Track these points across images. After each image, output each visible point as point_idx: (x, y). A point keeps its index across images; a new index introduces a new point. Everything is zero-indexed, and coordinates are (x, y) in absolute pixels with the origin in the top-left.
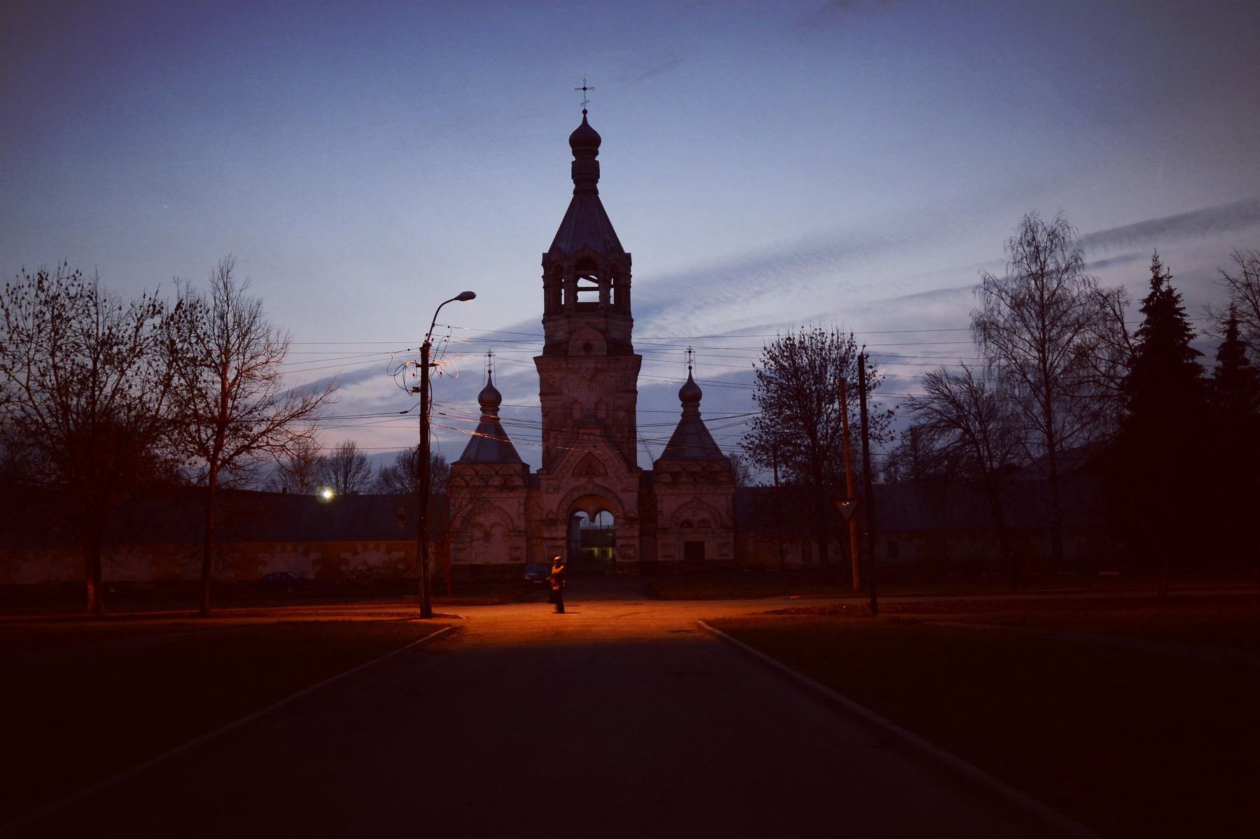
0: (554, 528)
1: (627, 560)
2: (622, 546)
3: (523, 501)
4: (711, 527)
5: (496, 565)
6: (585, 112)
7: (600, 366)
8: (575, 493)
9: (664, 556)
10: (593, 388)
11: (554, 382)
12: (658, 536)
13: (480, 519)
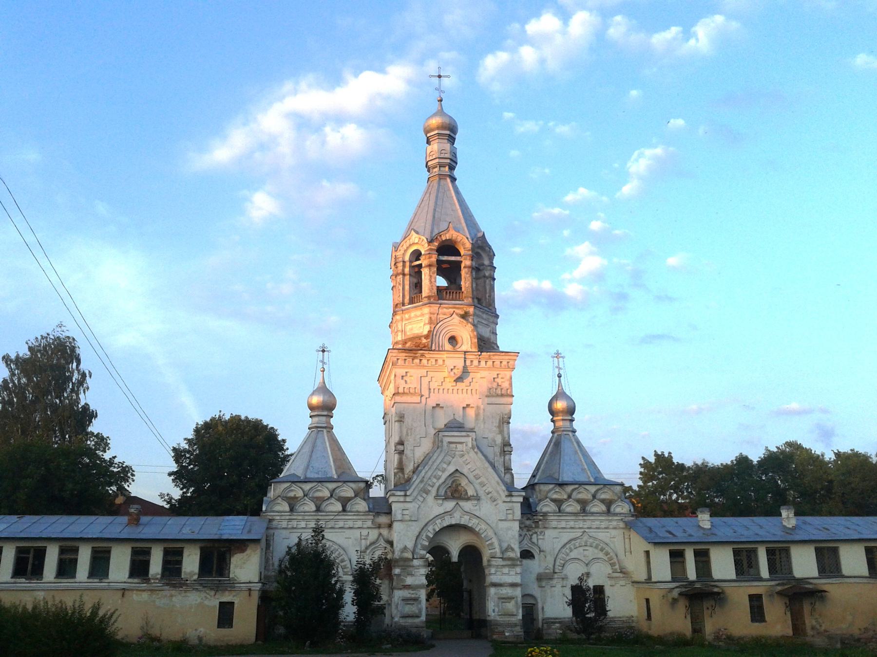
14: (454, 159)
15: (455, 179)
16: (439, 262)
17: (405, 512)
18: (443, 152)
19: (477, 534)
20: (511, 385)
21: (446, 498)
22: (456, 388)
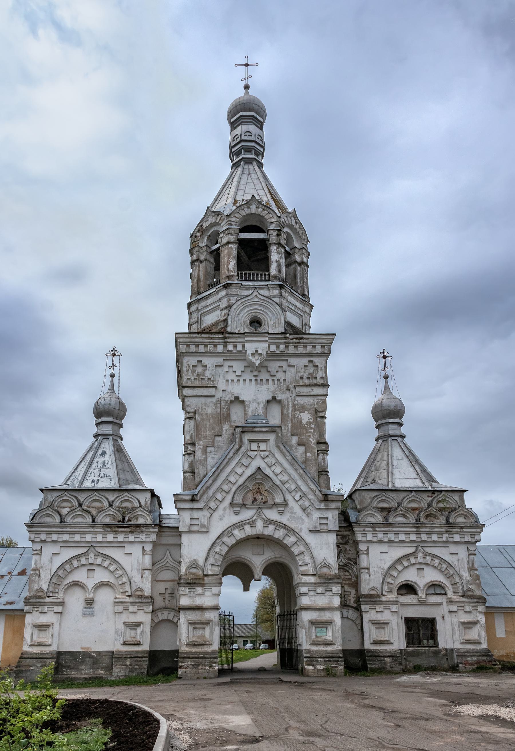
0: (199, 590)
1: (322, 648)
2: (313, 622)
3: (149, 548)
4: (445, 594)
5: (99, 653)
7: (273, 348)
9: (376, 642)
10: (262, 380)
11: (205, 371)
12: (363, 607)
13: (80, 576)
14: (260, 142)
15: (262, 165)
17: (195, 522)
18: (248, 134)
19: (286, 548)
20: (326, 372)
21: (243, 505)
22: (259, 379)
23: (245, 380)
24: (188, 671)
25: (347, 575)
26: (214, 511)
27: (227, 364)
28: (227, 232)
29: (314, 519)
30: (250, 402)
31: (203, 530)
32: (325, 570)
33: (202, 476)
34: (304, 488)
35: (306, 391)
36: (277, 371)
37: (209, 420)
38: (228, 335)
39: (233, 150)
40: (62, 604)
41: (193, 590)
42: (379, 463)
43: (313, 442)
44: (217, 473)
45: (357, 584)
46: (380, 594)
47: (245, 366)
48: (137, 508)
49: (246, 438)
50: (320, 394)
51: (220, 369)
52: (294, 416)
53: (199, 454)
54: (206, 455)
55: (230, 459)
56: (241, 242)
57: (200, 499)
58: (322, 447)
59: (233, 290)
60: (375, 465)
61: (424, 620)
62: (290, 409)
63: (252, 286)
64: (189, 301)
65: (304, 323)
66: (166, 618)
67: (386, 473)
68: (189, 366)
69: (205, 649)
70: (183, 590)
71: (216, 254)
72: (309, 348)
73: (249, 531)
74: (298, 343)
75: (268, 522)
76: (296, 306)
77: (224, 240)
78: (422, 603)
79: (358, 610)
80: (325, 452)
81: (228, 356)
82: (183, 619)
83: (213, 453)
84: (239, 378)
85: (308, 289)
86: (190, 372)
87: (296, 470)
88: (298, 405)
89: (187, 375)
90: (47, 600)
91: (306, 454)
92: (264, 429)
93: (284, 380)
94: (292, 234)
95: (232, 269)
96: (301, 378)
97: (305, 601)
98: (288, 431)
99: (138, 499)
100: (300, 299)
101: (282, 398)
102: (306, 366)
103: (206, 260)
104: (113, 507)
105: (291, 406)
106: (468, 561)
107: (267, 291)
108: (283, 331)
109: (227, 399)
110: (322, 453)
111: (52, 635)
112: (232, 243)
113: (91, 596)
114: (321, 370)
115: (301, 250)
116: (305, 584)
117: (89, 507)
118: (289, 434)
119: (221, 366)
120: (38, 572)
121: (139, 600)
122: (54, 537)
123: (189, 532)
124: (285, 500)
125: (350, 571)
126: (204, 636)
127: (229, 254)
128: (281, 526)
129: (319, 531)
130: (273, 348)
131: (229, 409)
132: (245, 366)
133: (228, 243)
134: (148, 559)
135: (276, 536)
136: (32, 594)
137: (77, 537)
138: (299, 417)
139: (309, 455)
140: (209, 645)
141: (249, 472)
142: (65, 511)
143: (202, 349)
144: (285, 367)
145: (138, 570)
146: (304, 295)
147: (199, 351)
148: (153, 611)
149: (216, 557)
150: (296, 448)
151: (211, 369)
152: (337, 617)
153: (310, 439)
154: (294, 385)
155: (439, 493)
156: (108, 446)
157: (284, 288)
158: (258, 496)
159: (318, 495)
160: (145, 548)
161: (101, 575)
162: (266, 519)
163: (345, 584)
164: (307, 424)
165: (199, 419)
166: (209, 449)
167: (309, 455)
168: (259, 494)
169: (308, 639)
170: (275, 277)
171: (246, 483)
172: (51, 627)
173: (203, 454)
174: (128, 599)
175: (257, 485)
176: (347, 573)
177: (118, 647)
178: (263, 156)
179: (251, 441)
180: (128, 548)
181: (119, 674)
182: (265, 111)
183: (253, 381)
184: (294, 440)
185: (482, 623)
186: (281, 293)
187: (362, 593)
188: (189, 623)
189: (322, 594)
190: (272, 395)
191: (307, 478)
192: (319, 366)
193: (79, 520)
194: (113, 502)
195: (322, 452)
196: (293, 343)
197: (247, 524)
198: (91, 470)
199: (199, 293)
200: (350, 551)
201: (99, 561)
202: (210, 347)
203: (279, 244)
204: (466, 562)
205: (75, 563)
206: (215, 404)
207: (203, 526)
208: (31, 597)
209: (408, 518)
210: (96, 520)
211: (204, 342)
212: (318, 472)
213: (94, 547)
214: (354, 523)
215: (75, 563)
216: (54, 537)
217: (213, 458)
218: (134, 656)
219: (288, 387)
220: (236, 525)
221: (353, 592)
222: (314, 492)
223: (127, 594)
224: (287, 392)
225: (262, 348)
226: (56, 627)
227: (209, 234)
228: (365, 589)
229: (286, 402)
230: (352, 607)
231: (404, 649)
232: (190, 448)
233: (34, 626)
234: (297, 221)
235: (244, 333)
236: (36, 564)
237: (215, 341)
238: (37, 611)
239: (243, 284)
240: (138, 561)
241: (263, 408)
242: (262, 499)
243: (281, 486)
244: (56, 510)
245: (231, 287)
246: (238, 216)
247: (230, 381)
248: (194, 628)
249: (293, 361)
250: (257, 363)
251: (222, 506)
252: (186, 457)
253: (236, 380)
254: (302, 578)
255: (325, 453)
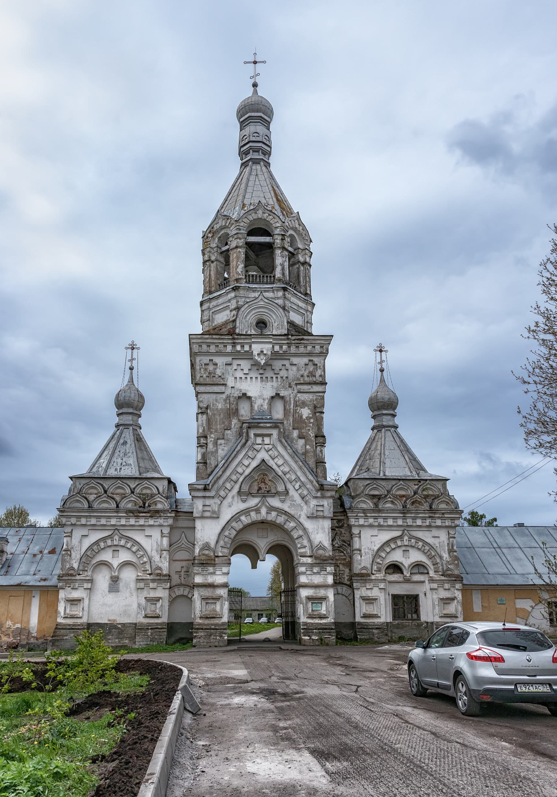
0: (211, 569)
2: (309, 598)
3: (166, 531)
5: (124, 625)
6: (255, 85)
7: (277, 348)
8: (243, 518)
10: (267, 378)
11: (215, 369)
13: (106, 556)
14: (267, 143)
16: (247, 243)
20: (324, 371)
21: (250, 494)
23: (251, 378)
24: (202, 640)
25: (342, 556)
26: (224, 498)
27: (236, 362)
28: (235, 236)
29: (312, 506)
30: (256, 398)
31: (215, 516)
32: (321, 552)
33: (213, 466)
34: (303, 479)
35: (305, 388)
36: (280, 370)
37: (220, 415)
38: (236, 337)
39: (242, 150)
40: (91, 581)
41: (206, 569)
42: (373, 452)
43: (312, 435)
44: (226, 465)
45: (351, 564)
46: (370, 573)
47: (251, 365)
48: (156, 495)
49: (252, 433)
50: (319, 391)
51: (229, 368)
52: (295, 411)
53: (210, 446)
54: (217, 447)
55: (238, 452)
56: (249, 245)
57: (211, 488)
58: (321, 440)
59: (242, 292)
60: (370, 454)
61: (408, 596)
62: (292, 405)
63: (258, 289)
64: (201, 299)
65: (306, 321)
66: (182, 594)
67: (379, 462)
68: (202, 365)
69: (216, 621)
70: (196, 569)
71: (226, 255)
72: (309, 348)
73: (254, 516)
74: (299, 343)
75: (271, 509)
76: (298, 306)
77: (234, 244)
78: (407, 581)
79: (351, 587)
80: (323, 445)
81: (236, 355)
82: (197, 595)
83: (223, 445)
84: (246, 376)
85: (310, 288)
86: (202, 370)
87: (296, 462)
88: (299, 401)
89: (200, 373)
90: (78, 577)
91: (306, 446)
92: (268, 425)
93: (287, 377)
94: (296, 235)
95: (240, 272)
96: (302, 376)
97: (303, 579)
98: (290, 425)
99: (156, 486)
100: (302, 299)
101: (285, 395)
102: (306, 365)
103: (217, 260)
104: (135, 494)
105: (292, 402)
106: (448, 544)
107: (272, 294)
108: (286, 332)
109: (235, 395)
110: (320, 446)
111: (83, 609)
112: (240, 247)
113: (116, 574)
114: (320, 368)
115: (304, 251)
116: (303, 564)
117: (113, 494)
118: (291, 428)
119: (230, 364)
120: (69, 553)
121: (159, 578)
122: (83, 521)
123: (202, 517)
124: (286, 489)
125: (345, 552)
126: (215, 611)
127: (238, 258)
128: (283, 513)
129: (317, 517)
130: (277, 348)
131: (237, 404)
132: (251, 365)
133: (237, 247)
134: (165, 541)
135: (278, 522)
136: (64, 572)
137: (103, 521)
138: (300, 412)
139: (308, 447)
140: (219, 618)
141: (254, 464)
142: (92, 498)
143: (213, 349)
144: (288, 365)
145: (157, 551)
146: (306, 294)
147: (210, 351)
148: (170, 588)
149: (225, 540)
150: (297, 441)
151: (221, 367)
152: (330, 594)
153: (310, 433)
154: (295, 382)
155: (424, 482)
156: (128, 435)
157: (287, 291)
158: (262, 485)
159: (315, 485)
160: (163, 531)
161: (124, 556)
162: (270, 507)
163: (340, 563)
164: (307, 419)
165: (211, 414)
166: (220, 442)
167: (308, 447)
168: (263, 484)
169: (305, 613)
170: (280, 280)
171: (252, 474)
172: (82, 602)
173: (214, 446)
174: (148, 577)
175: (262, 476)
176: (342, 554)
177: (141, 620)
178: (269, 154)
179: (256, 435)
180: (148, 532)
181: (141, 643)
182: (272, 111)
183: (259, 378)
184: (295, 433)
185: (459, 599)
186: (284, 295)
187: (355, 572)
188: (202, 599)
189: (318, 573)
190: (276, 392)
191: (305, 469)
192: (318, 365)
193: (105, 505)
194: (134, 489)
195: (320, 444)
196: (294, 344)
197: (252, 511)
198: (114, 459)
199: (211, 293)
200: (345, 533)
201: (122, 542)
202: (220, 347)
203: (284, 248)
204: (446, 544)
205: (102, 545)
206: (225, 400)
207: (214, 512)
208: (64, 575)
209: (396, 504)
210: (120, 505)
211: (215, 343)
212: (317, 463)
213: (118, 530)
214: (348, 509)
215: (102, 545)
216: (83, 521)
217: (223, 450)
218: (154, 628)
219: (290, 384)
220: (243, 512)
221: (347, 570)
222: (311, 482)
223: (148, 573)
224: (290, 388)
225: (267, 348)
226: (86, 602)
227: (219, 236)
228: (357, 568)
229: (288, 399)
230: (346, 584)
231: (390, 622)
232: (202, 441)
233: (67, 600)
234: (301, 223)
235: (251, 335)
236: (67, 545)
237: (225, 341)
238: (69, 587)
239: (250, 287)
240: (157, 542)
241: (267, 403)
242: (266, 488)
243: (283, 476)
244: (83, 497)
245: (239, 290)
246: (246, 222)
247: (238, 379)
248: (207, 603)
249: (295, 360)
250: (263, 362)
251: (230, 495)
252: (199, 449)
253: (243, 378)
254: (300, 559)
255: (323, 446)
